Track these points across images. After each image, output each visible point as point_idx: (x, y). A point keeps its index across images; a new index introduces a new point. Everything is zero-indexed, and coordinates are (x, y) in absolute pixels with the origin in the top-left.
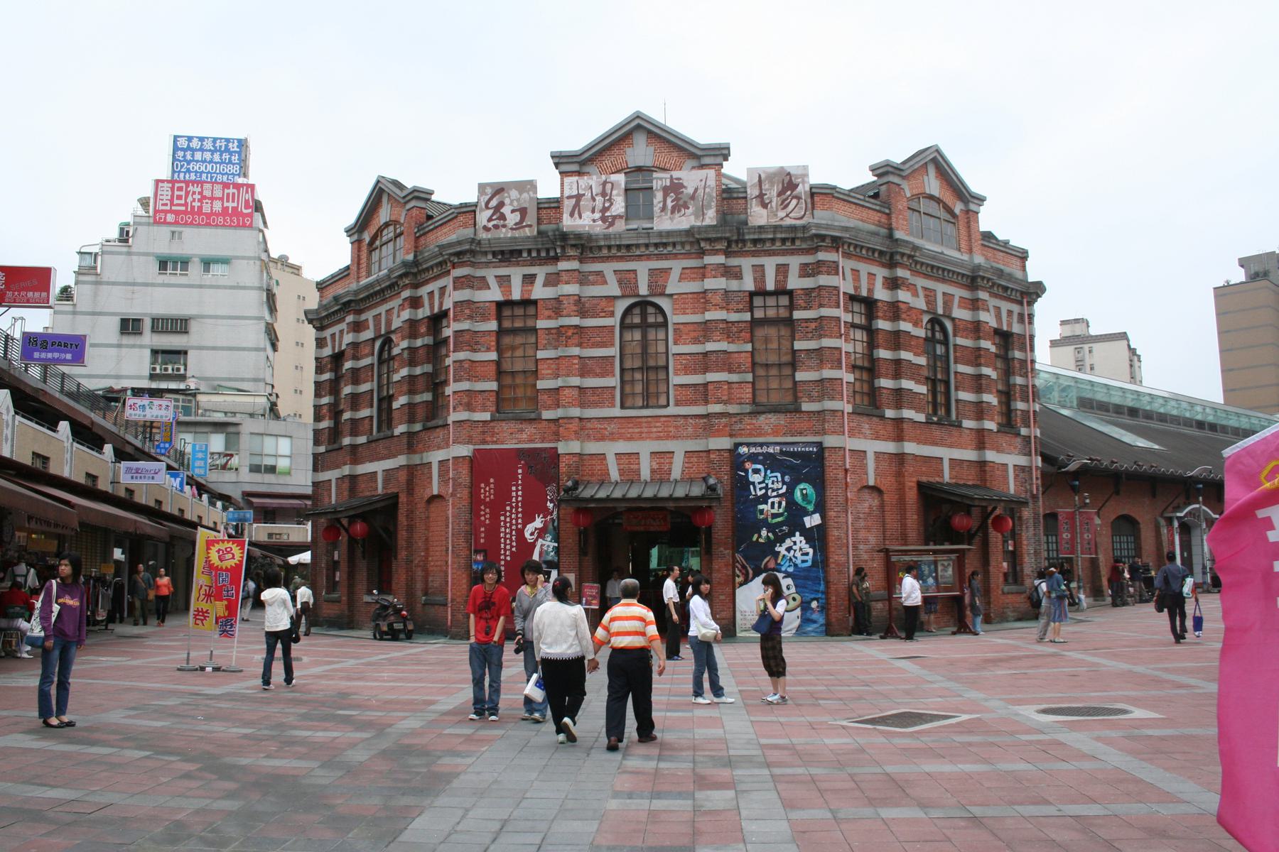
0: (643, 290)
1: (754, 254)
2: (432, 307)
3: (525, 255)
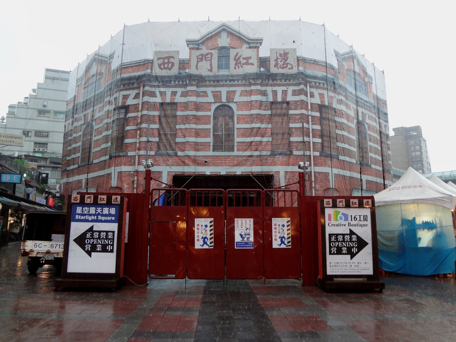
0: (224, 100)
3: (173, 83)
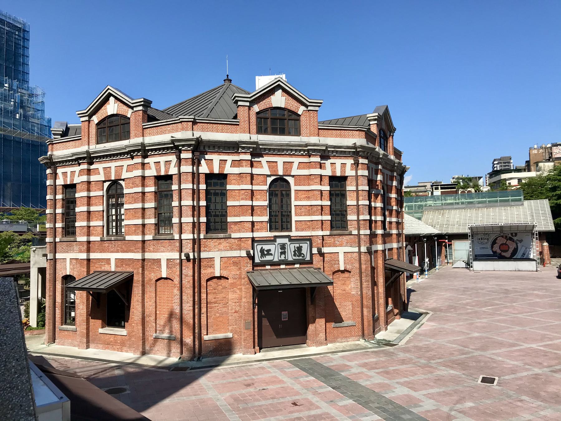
2: (158, 170)
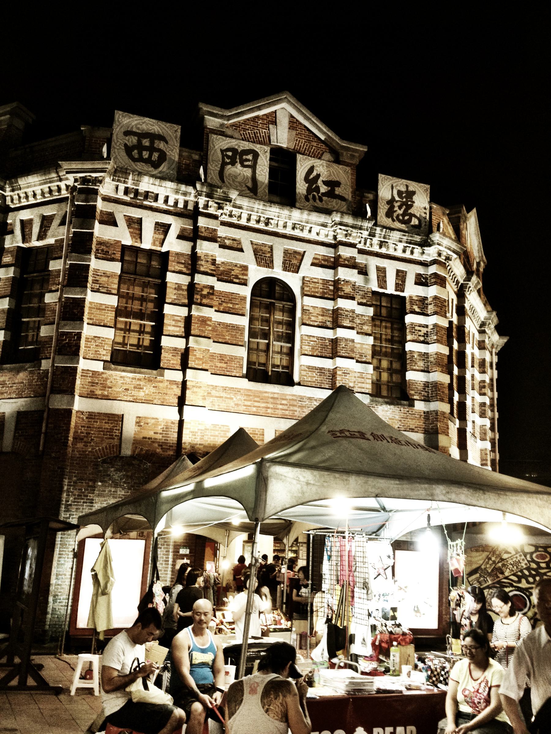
1: (378, 255)
3: (161, 199)
